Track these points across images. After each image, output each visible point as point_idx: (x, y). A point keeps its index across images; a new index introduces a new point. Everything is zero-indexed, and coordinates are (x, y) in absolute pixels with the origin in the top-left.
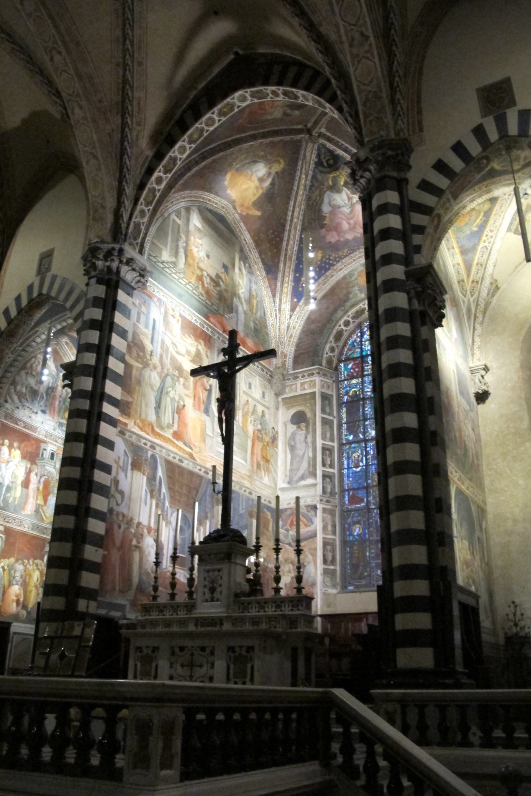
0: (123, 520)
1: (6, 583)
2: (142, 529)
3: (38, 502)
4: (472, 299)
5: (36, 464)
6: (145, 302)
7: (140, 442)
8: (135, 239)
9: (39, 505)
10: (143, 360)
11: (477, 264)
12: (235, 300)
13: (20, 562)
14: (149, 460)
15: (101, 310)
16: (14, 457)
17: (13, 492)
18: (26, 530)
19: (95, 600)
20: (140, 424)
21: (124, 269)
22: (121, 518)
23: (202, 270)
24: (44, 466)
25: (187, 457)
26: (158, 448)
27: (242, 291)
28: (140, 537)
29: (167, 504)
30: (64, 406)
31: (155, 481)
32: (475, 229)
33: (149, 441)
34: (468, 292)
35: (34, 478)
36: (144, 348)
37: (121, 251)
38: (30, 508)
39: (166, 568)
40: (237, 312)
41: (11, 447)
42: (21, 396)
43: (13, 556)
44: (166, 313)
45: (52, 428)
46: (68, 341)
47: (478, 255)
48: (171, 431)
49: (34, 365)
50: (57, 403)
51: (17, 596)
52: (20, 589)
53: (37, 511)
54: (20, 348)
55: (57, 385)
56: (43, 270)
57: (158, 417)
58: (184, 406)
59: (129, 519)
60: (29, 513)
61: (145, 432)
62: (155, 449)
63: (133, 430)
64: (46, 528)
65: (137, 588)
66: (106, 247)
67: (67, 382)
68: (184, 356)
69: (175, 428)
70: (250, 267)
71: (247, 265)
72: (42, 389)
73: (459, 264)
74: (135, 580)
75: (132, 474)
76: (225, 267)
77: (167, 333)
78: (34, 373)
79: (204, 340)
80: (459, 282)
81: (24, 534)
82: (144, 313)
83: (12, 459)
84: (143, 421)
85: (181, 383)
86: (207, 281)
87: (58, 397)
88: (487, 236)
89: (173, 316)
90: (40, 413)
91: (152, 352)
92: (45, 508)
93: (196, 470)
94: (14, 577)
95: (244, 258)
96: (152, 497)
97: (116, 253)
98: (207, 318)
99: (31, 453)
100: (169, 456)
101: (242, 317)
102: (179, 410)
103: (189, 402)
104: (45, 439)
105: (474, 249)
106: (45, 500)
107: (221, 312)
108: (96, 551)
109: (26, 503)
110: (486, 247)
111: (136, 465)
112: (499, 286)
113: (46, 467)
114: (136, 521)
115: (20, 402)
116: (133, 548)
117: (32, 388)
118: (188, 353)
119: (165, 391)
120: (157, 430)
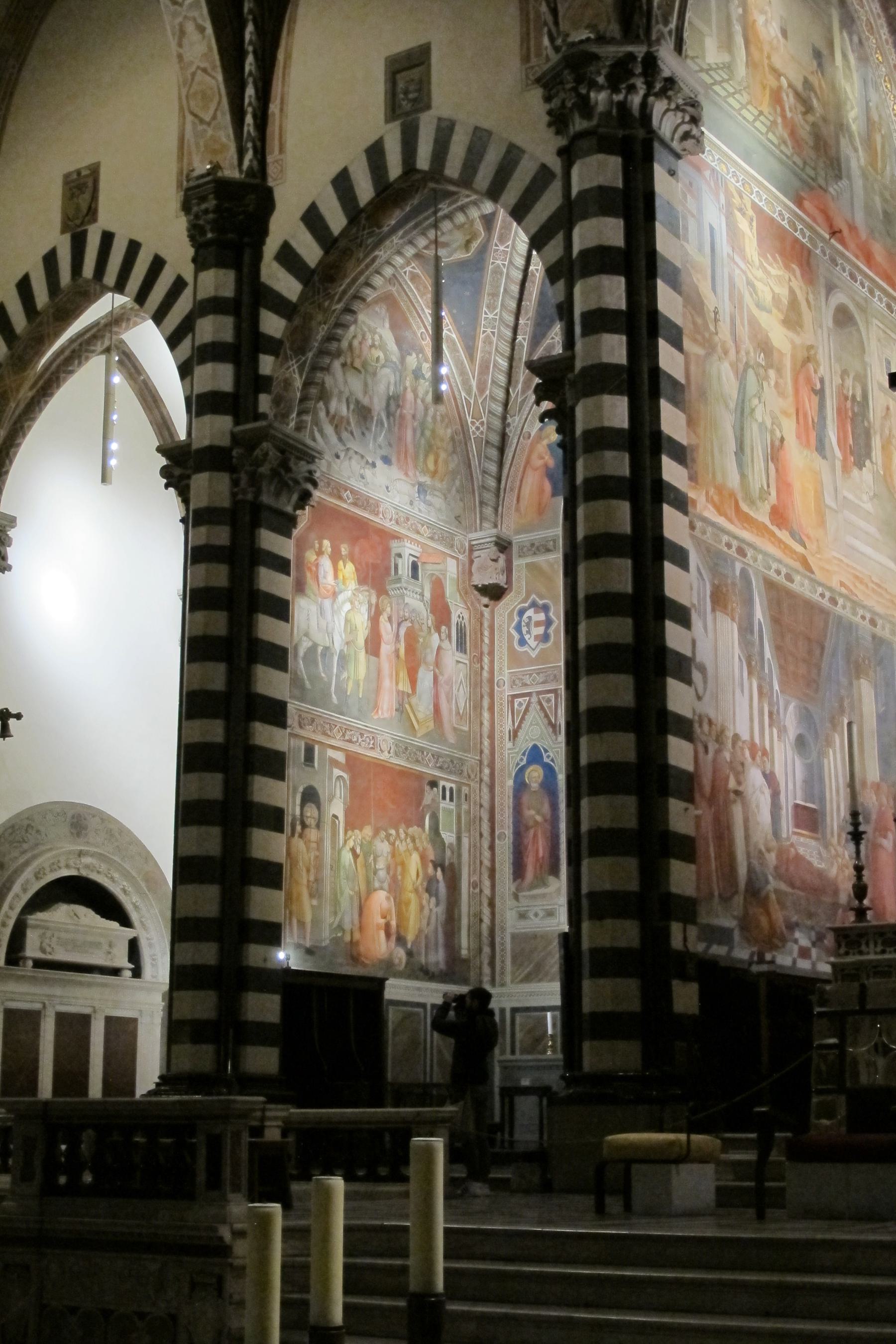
0: (710, 733)
1: (363, 887)
2: (742, 749)
3: (401, 687)
5: (387, 593)
6: (691, 184)
7: (721, 541)
8: (666, 22)
9: (403, 692)
10: (704, 337)
12: (844, 142)
13: (383, 834)
14: (738, 581)
15: (621, 222)
16: (344, 583)
17: (351, 667)
18: (385, 756)
19: (694, 922)
20: (716, 498)
21: (659, 107)
22: (706, 727)
23: (777, 74)
24: (402, 596)
25: (797, 565)
26: (750, 553)
27: (853, 115)
28: (740, 768)
29: (776, 687)
30: (423, 441)
31: (752, 632)
33: (736, 537)
35: (386, 629)
36: (702, 303)
37: (651, 64)
38: (387, 703)
39: (788, 838)
40: (849, 178)
41: (335, 557)
42: (338, 424)
43: (369, 823)
44: (729, 204)
45: (406, 499)
46: (418, 271)
48: (766, 508)
49: (356, 343)
50: (409, 434)
51: (384, 917)
52: (388, 898)
53: (401, 710)
54: (339, 306)
55: (405, 389)
56: (406, 106)
57: (743, 476)
58: (782, 440)
59: (719, 730)
60: (386, 715)
61: (726, 516)
62: (745, 556)
63: (706, 514)
64: (422, 750)
65: (747, 891)
66: (612, 52)
67: (546, 405)
68: (769, 312)
69: (773, 497)
70: (860, 42)
71: (855, 39)
72: (378, 406)
74: (742, 871)
75: (715, 619)
76: (817, 55)
77: (737, 259)
78: (357, 364)
79: (801, 266)
81: (382, 767)
82: (693, 216)
83: (341, 585)
84: (720, 489)
85: (772, 383)
86: (789, 100)
87: (409, 417)
89: (740, 210)
90: (379, 463)
91: (716, 313)
92: (414, 700)
93: (816, 597)
94: (375, 872)
95: (849, 21)
96: (750, 673)
97: (638, 70)
98: (799, 202)
99: (375, 567)
100: (770, 568)
101: (858, 183)
102: (775, 453)
103: (789, 428)
104: (397, 528)
106: (413, 682)
107: (821, 181)
108: (686, 809)
109: (378, 690)
111: (719, 599)
113: (407, 600)
114: (730, 734)
115: (340, 439)
116: (732, 796)
117: (357, 402)
118: (776, 299)
119: (747, 410)
120: (744, 507)
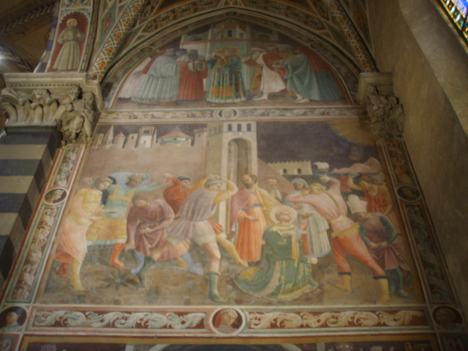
4: (330, 23)
34: (322, 19)
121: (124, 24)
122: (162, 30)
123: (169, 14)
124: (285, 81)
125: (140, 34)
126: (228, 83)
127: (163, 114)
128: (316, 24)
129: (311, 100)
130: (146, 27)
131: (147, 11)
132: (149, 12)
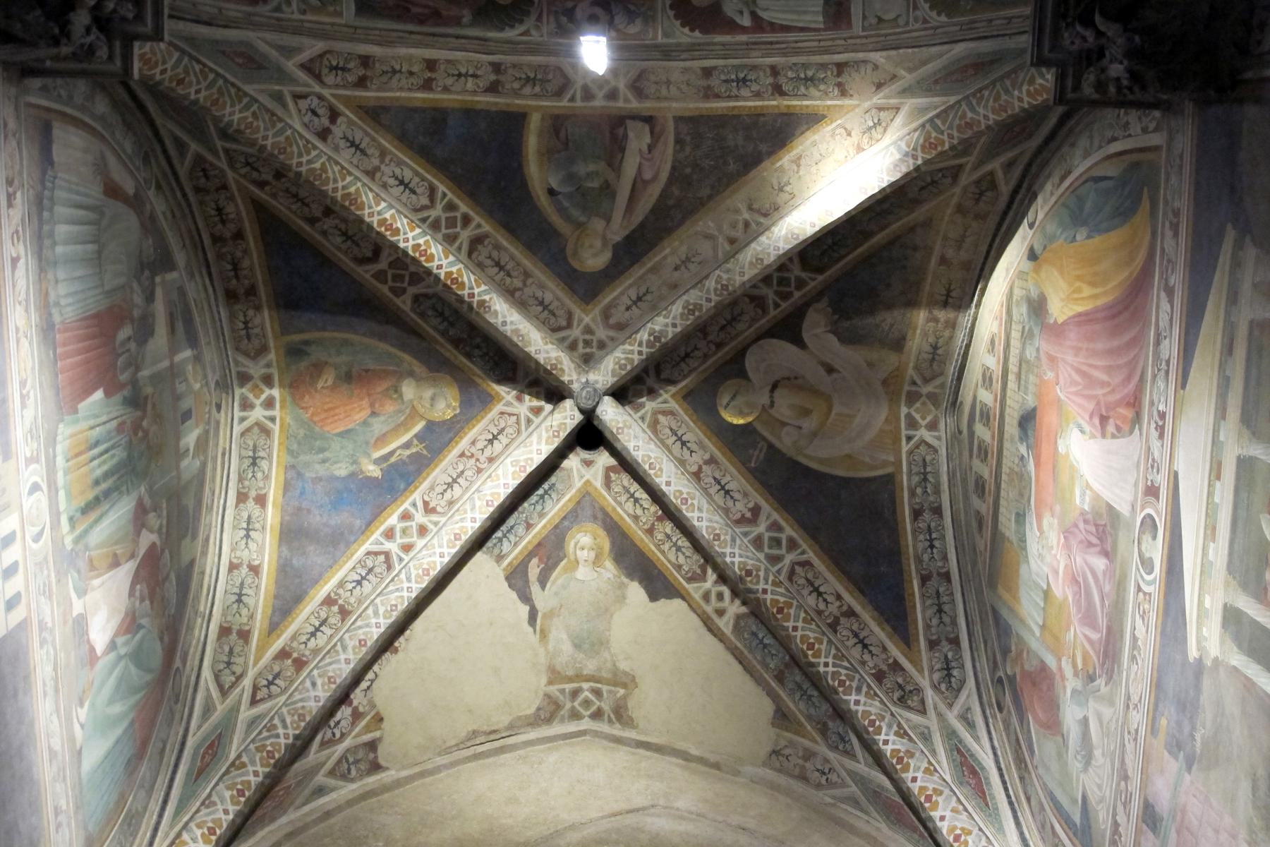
4: (245, 714)
11: (329, 601)
32: (373, 471)
34: (247, 683)
47: (344, 570)
73: (255, 570)
80: (224, 631)
88: (406, 516)
105: (339, 541)
110: (387, 555)
112: (383, 754)
121: (246, 118)
122: (189, 206)
123: (233, 226)
124: (112, 646)
125: (194, 147)
126: (99, 472)
127: (23, 296)
128: (229, 664)
129: (80, 753)
130: (211, 164)
131: (259, 171)
132: (255, 174)
